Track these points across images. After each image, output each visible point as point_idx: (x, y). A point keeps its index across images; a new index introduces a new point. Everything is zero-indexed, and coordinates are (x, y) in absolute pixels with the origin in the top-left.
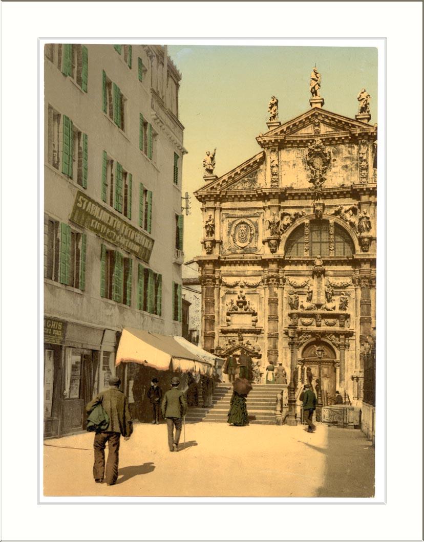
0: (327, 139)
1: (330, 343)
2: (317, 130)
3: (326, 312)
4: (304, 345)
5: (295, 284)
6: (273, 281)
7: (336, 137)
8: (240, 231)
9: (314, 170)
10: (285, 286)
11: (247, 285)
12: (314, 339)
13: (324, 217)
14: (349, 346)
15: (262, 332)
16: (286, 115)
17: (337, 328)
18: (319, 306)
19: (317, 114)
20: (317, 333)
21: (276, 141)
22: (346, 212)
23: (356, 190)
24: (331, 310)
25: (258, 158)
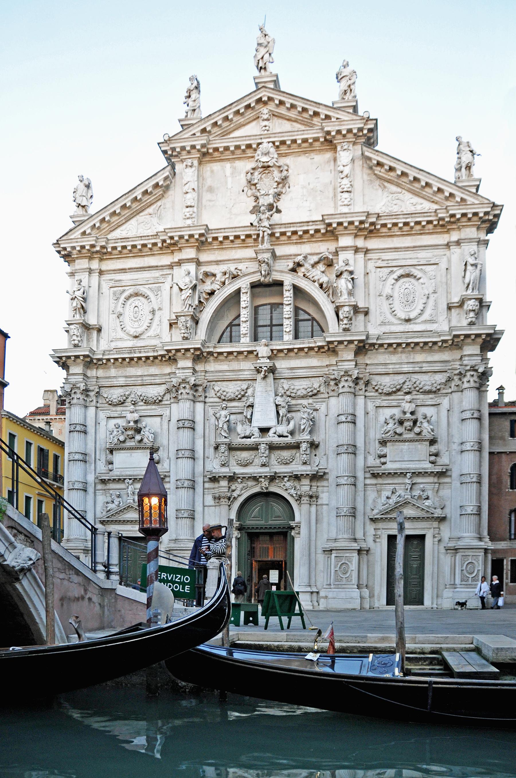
0: (283, 143)
2: (266, 126)
3: (276, 440)
5: (225, 393)
6: (184, 388)
7: (299, 139)
9: (258, 194)
10: (207, 400)
13: (276, 276)
14: (317, 497)
16: (210, 103)
18: (264, 431)
19: (265, 99)
22: (313, 266)
24: (287, 437)
25: (160, 179)
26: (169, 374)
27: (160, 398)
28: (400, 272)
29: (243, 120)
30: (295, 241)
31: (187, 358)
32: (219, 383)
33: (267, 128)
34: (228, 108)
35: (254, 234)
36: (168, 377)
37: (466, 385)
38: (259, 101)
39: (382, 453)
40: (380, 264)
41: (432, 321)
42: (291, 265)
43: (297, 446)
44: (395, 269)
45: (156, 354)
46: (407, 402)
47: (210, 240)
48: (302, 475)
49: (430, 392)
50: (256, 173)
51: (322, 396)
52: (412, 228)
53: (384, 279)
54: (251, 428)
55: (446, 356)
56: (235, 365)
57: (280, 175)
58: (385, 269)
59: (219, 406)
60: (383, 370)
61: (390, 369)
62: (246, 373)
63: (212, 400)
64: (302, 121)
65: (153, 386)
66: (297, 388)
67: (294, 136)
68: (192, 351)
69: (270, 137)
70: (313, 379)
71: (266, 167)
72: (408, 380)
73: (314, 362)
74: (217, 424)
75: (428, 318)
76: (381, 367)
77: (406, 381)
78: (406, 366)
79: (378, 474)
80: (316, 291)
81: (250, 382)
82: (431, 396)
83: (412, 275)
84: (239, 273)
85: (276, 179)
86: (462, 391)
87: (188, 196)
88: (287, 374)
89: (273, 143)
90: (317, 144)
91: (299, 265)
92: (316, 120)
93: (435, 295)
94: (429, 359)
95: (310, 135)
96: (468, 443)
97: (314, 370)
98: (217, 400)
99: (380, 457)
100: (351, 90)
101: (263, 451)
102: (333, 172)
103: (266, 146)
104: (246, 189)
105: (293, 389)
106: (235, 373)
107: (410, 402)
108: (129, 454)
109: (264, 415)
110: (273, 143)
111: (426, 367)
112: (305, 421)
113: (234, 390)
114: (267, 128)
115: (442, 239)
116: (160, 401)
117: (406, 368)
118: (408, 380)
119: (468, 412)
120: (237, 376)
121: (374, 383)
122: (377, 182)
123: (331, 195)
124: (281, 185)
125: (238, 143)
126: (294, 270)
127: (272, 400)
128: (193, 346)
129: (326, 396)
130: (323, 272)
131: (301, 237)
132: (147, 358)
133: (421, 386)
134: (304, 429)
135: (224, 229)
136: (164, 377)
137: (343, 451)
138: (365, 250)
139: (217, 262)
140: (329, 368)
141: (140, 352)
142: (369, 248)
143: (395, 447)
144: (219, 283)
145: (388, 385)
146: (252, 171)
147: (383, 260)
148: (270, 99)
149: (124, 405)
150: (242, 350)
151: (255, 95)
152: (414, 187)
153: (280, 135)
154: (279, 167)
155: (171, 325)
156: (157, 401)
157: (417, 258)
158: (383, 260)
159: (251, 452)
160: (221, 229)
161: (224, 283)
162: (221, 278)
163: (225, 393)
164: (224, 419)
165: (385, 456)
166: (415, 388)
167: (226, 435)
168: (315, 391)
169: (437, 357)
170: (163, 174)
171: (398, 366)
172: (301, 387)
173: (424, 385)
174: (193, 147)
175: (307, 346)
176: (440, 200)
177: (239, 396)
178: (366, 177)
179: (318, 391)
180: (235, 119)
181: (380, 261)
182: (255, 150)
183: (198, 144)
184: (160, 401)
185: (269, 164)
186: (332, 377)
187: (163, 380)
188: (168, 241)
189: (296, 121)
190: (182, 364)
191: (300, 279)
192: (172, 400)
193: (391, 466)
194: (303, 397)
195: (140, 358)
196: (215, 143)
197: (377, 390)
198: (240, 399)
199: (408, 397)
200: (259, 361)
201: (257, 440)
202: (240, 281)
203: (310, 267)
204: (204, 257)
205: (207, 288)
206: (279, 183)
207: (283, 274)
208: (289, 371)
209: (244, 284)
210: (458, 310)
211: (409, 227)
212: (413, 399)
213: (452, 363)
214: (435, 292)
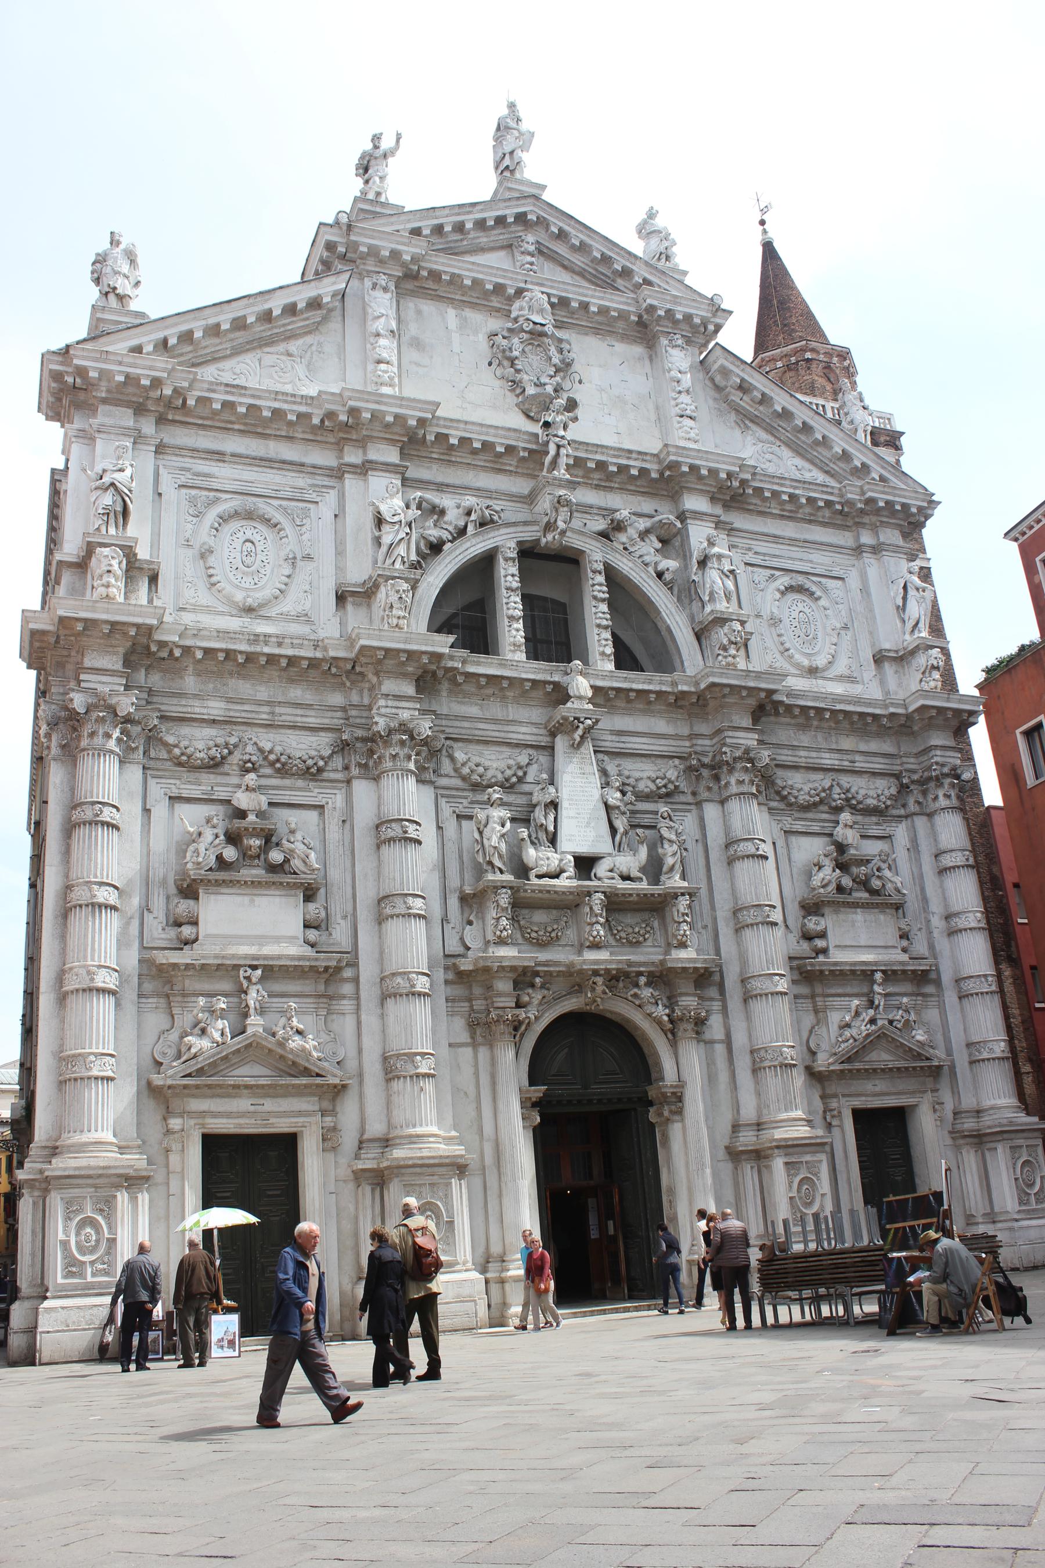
1: (637, 1018)
2: (532, 264)
4: (539, 1027)
5: (481, 769)
6: (402, 743)
8: (238, 544)
11: (272, 764)
12: (571, 1004)
15: (348, 973)
17: (648, 955)
18: (585, 864)
19: (532, 217)
20: (596, 973)
21: (395, 254)
22: (644, 535)
23: (674, 466)
26: (344, 709)
27: (321, 763)
28: (784, 581)
29: (485, 240)
30: (595, 482)
31: (405, 675)
32: (460, 744)
33: (535, 267)
34: (468, 209)
35: (525, 449)
36: (339, 714)
37: (943, 802)
38: (521, 218)
39: (819, 928)
40: (750, 558)
41: (850, 679)
42: (601, 525)
43: (656, 907)
44: (778, 573)
45: (319, 655)
46: (846, 825)
47: (430, 437)
48: (684, 969)
49: (874, 811)
50: (516, 340)
51: (682, 798)
52: (801, 506)
53: (762, 587)
54: (558, 856)
55: (887, 746)
56: (495, 709)
57: (558, 355)
58: (761, 570)
59: (466, 798)
60: (790, 758)
61: (802, 757)
62: (523, 729)
63: (443, 782)
64: (595, 276)
65: (298, 732)
66: (637, 775)
67: (586, 296)
68: (425, 660)
69: (542, 285)
70: (659, 761)
71: (537, 335)
72: (834, 783)
73: (661, 725)
74: (477, 836)
75: (847, 672)
76: (786, 752)
77: (832, 786)
78: (827, 755)
79: (822, 972)
80: (651, 583)
81: (531, 751)
82: (874, 819)
83: (807, 590)
84: (496, 518)
85: (556, 360)
86: (930, 815)
87: (383, 342)
88: (610, 743)
89: (549, 295)
90: (621, 324)
91: (619, 527)
92: (620, 283)
93: (849, 633)
94: (863, 747)
95: (616, 302)
96: (971, 915)
97: (663, 742)
98: (457, 782)
99: (808, 937)
100: (668, 258)
101: (597, 909)
102: (651, 379)
103: (537, 295)
104: (495, 363)
105: (628, 777)
106: (500, 727)
107: (851, 827)
108: (246, 899)
109: (581, 829)
110: (549, 295)
111: (861, 763)
112: (675, 847)
113: (502, 765)
114: (535, 267)
115: (844, 538)
116: (320, 770)
117: (828, 760)
118: (834, 783)
119: (959, 854)
120: (502, 735)
121: (779, 782)
122: (733, 416)
123: (653, 417)
124: (562, 374)
125: (480, 276)
126: (604, 535)
127: (596, 792)
128: (430, 649)
129: (690, 798)
130: (657, 551)
131: (610, 476)
132: (292, 661)
133: (860, 797)
134: (673, 866)
135: (466, 423)
136: (330, 714)
137: (760, 919)
138: (729, 527)
139: (441, 487)
140: (695, 742)
141: (280, 645)
142: (735, 525)
143: (841, 916)
144: (451, 528)
145: (806, 789)
146: (506, 334)
147: (756, 553)
148: (541, 222)
149: (226, 768)
150: (524, 676)
151: (517, 206)
152: (798, 438)
153: (561, 286)
154: (560, 341)
155: (341, 598)
156: (314, 770)
157: (811, 562)
158: (756, 553)
159: (554, 912)
160: (458, 421)
161: (462, 532)
162: (457, 519)
163: (481, 769)
164: (499, 828)
165: (823, 935)
166: (847, 800)
167: (503, 868)
168: (671, 786)
169: (873, 746)
170: (334, 283)
171: (814, 754)
172: (645, 775)
173: (866, 796)
174: (395, 254)
175: (658, 688)
176: (841, 472)
177: (514, 779)
178: (711, 402)
179: (676, 787)
180: (472, 235)
181: (750, 554)
182: (510, 300)
183: (407, 252)
184: (320, 770)
185: (546, 328)
186: (706, 760)
187: (327, 721)
188: (343, 418)
189: (582, 274)
190: (389, 686)
191: (617, 555)
192: (355, 771)
193: (839, 957)
194: (647, 797)
195: (272, 659)
196: (436, 263)
197: (784, 798)
198: (512, 786)
199: (845, 817)
200: (569, 705)
201: (575, 883)
202: (497, 533)
203: (636, 536)
204: (414, 472)
205: (430, 532)
206: (558, 370)
207: (581, 538)
208: (614, 738)
209: (505, 541)
210: (894, 667)
211: (794, 508)
212: (855, 823)
213: (904, 760)
214: (846, 628)
